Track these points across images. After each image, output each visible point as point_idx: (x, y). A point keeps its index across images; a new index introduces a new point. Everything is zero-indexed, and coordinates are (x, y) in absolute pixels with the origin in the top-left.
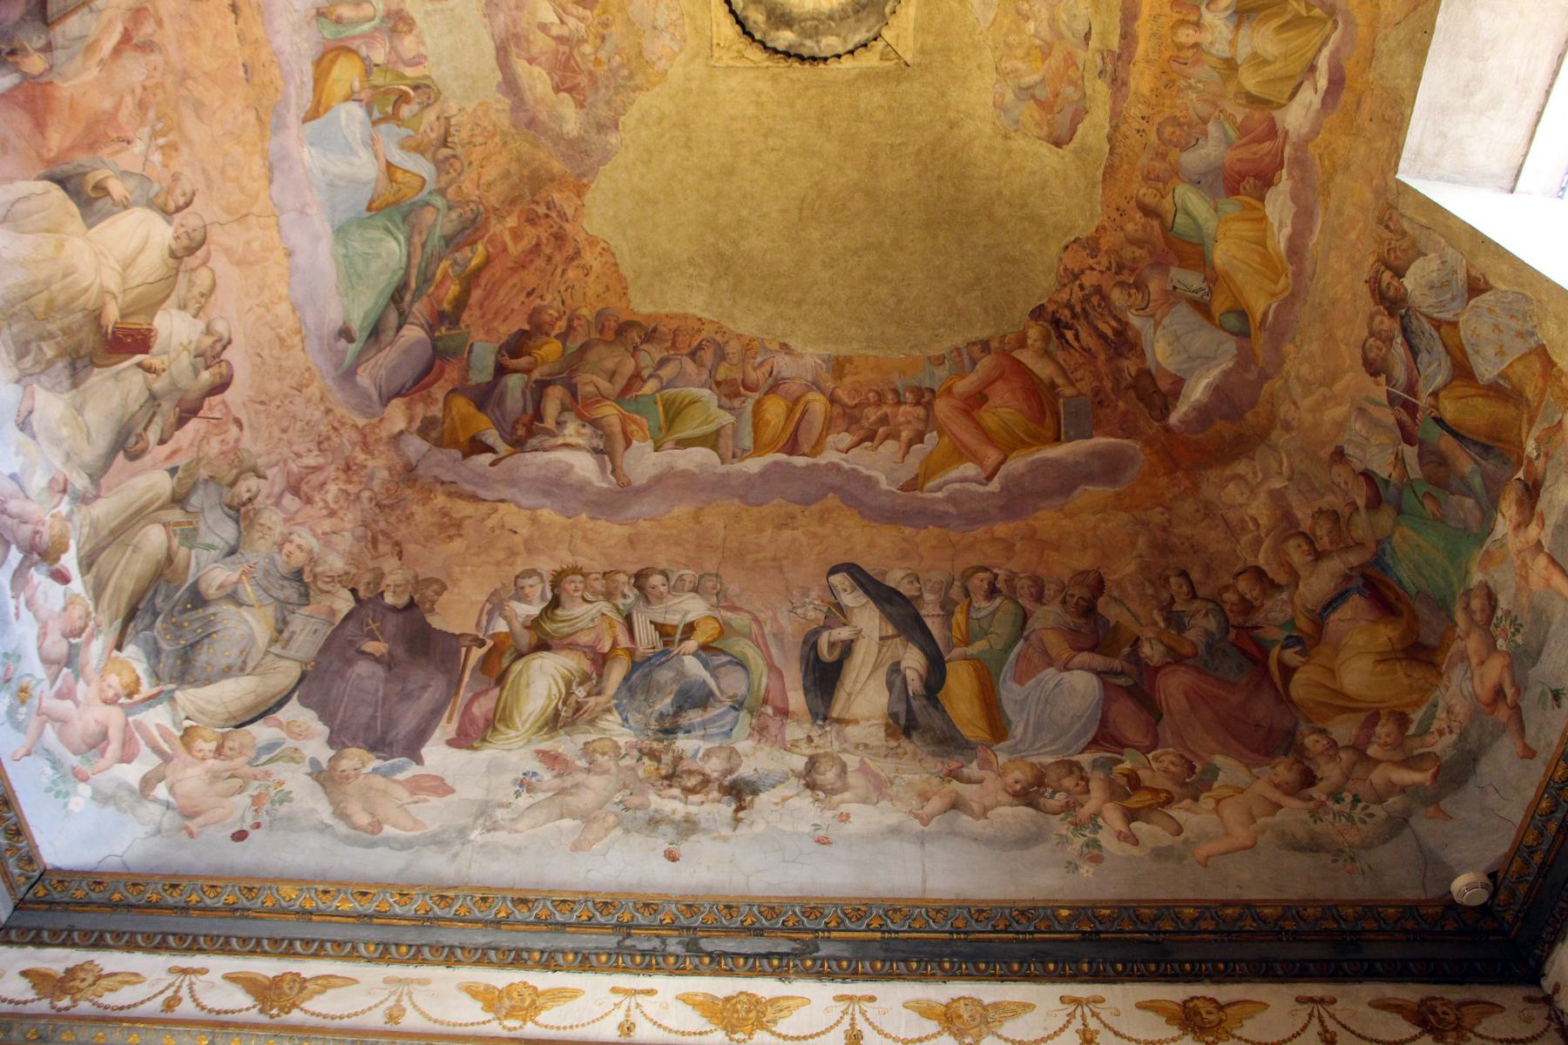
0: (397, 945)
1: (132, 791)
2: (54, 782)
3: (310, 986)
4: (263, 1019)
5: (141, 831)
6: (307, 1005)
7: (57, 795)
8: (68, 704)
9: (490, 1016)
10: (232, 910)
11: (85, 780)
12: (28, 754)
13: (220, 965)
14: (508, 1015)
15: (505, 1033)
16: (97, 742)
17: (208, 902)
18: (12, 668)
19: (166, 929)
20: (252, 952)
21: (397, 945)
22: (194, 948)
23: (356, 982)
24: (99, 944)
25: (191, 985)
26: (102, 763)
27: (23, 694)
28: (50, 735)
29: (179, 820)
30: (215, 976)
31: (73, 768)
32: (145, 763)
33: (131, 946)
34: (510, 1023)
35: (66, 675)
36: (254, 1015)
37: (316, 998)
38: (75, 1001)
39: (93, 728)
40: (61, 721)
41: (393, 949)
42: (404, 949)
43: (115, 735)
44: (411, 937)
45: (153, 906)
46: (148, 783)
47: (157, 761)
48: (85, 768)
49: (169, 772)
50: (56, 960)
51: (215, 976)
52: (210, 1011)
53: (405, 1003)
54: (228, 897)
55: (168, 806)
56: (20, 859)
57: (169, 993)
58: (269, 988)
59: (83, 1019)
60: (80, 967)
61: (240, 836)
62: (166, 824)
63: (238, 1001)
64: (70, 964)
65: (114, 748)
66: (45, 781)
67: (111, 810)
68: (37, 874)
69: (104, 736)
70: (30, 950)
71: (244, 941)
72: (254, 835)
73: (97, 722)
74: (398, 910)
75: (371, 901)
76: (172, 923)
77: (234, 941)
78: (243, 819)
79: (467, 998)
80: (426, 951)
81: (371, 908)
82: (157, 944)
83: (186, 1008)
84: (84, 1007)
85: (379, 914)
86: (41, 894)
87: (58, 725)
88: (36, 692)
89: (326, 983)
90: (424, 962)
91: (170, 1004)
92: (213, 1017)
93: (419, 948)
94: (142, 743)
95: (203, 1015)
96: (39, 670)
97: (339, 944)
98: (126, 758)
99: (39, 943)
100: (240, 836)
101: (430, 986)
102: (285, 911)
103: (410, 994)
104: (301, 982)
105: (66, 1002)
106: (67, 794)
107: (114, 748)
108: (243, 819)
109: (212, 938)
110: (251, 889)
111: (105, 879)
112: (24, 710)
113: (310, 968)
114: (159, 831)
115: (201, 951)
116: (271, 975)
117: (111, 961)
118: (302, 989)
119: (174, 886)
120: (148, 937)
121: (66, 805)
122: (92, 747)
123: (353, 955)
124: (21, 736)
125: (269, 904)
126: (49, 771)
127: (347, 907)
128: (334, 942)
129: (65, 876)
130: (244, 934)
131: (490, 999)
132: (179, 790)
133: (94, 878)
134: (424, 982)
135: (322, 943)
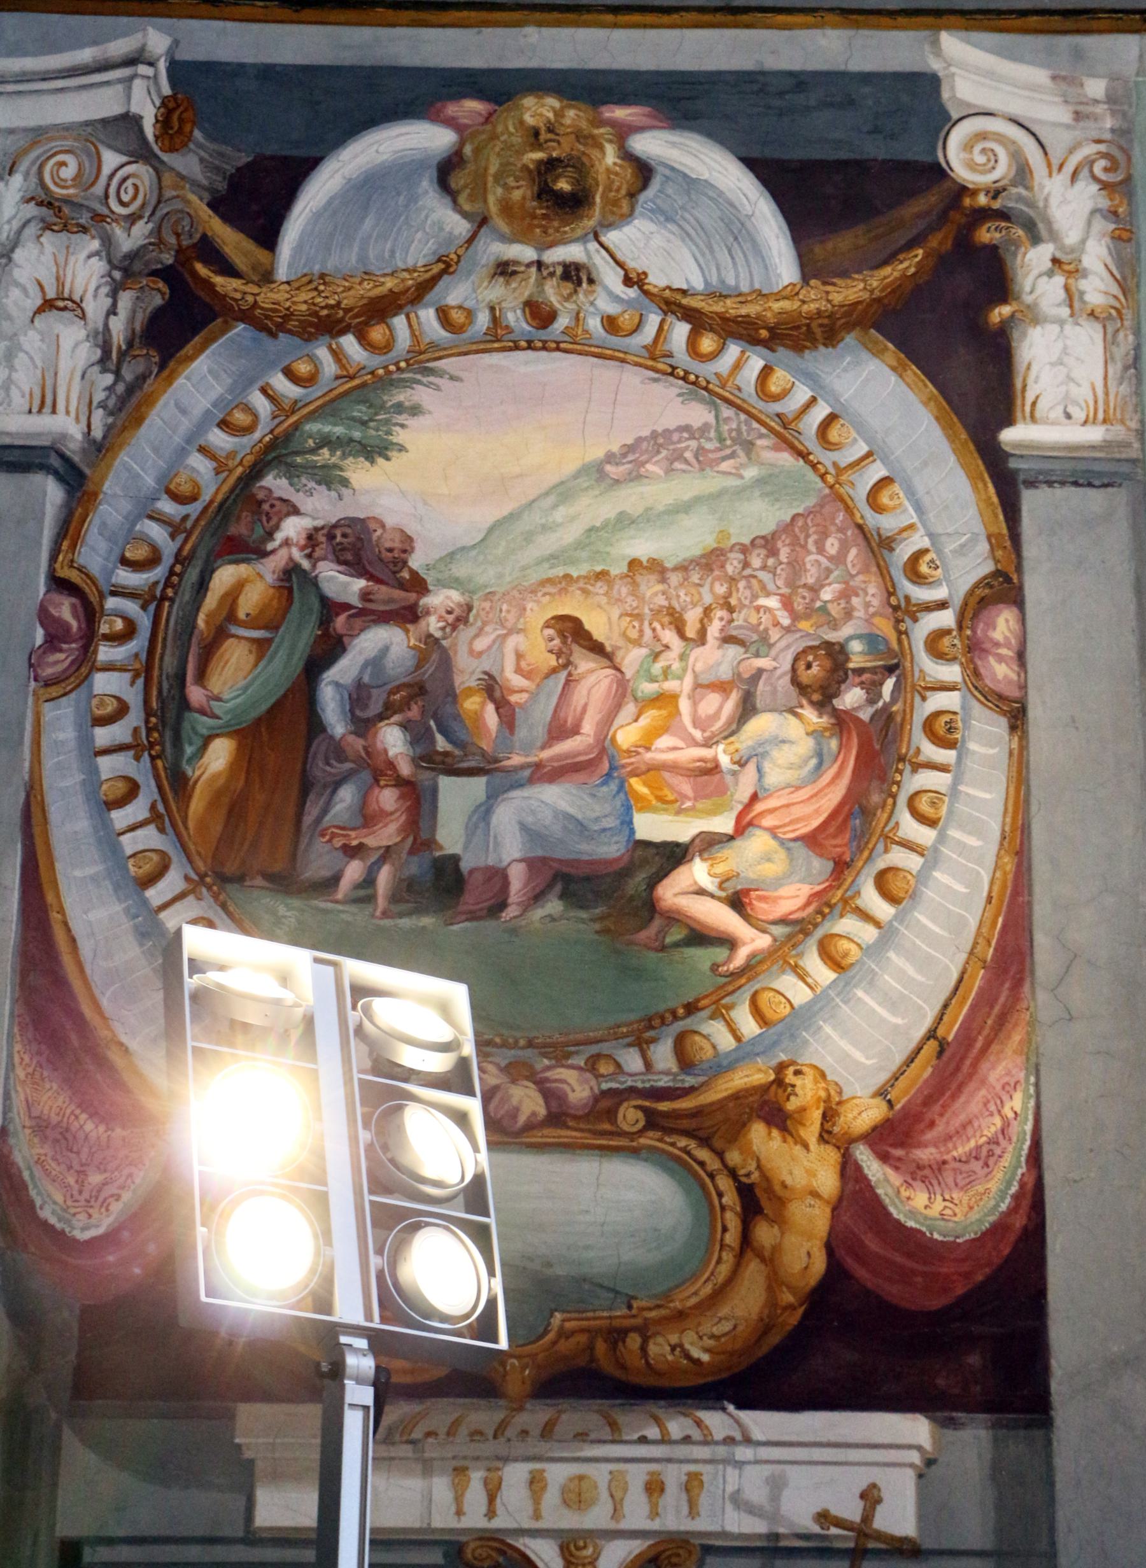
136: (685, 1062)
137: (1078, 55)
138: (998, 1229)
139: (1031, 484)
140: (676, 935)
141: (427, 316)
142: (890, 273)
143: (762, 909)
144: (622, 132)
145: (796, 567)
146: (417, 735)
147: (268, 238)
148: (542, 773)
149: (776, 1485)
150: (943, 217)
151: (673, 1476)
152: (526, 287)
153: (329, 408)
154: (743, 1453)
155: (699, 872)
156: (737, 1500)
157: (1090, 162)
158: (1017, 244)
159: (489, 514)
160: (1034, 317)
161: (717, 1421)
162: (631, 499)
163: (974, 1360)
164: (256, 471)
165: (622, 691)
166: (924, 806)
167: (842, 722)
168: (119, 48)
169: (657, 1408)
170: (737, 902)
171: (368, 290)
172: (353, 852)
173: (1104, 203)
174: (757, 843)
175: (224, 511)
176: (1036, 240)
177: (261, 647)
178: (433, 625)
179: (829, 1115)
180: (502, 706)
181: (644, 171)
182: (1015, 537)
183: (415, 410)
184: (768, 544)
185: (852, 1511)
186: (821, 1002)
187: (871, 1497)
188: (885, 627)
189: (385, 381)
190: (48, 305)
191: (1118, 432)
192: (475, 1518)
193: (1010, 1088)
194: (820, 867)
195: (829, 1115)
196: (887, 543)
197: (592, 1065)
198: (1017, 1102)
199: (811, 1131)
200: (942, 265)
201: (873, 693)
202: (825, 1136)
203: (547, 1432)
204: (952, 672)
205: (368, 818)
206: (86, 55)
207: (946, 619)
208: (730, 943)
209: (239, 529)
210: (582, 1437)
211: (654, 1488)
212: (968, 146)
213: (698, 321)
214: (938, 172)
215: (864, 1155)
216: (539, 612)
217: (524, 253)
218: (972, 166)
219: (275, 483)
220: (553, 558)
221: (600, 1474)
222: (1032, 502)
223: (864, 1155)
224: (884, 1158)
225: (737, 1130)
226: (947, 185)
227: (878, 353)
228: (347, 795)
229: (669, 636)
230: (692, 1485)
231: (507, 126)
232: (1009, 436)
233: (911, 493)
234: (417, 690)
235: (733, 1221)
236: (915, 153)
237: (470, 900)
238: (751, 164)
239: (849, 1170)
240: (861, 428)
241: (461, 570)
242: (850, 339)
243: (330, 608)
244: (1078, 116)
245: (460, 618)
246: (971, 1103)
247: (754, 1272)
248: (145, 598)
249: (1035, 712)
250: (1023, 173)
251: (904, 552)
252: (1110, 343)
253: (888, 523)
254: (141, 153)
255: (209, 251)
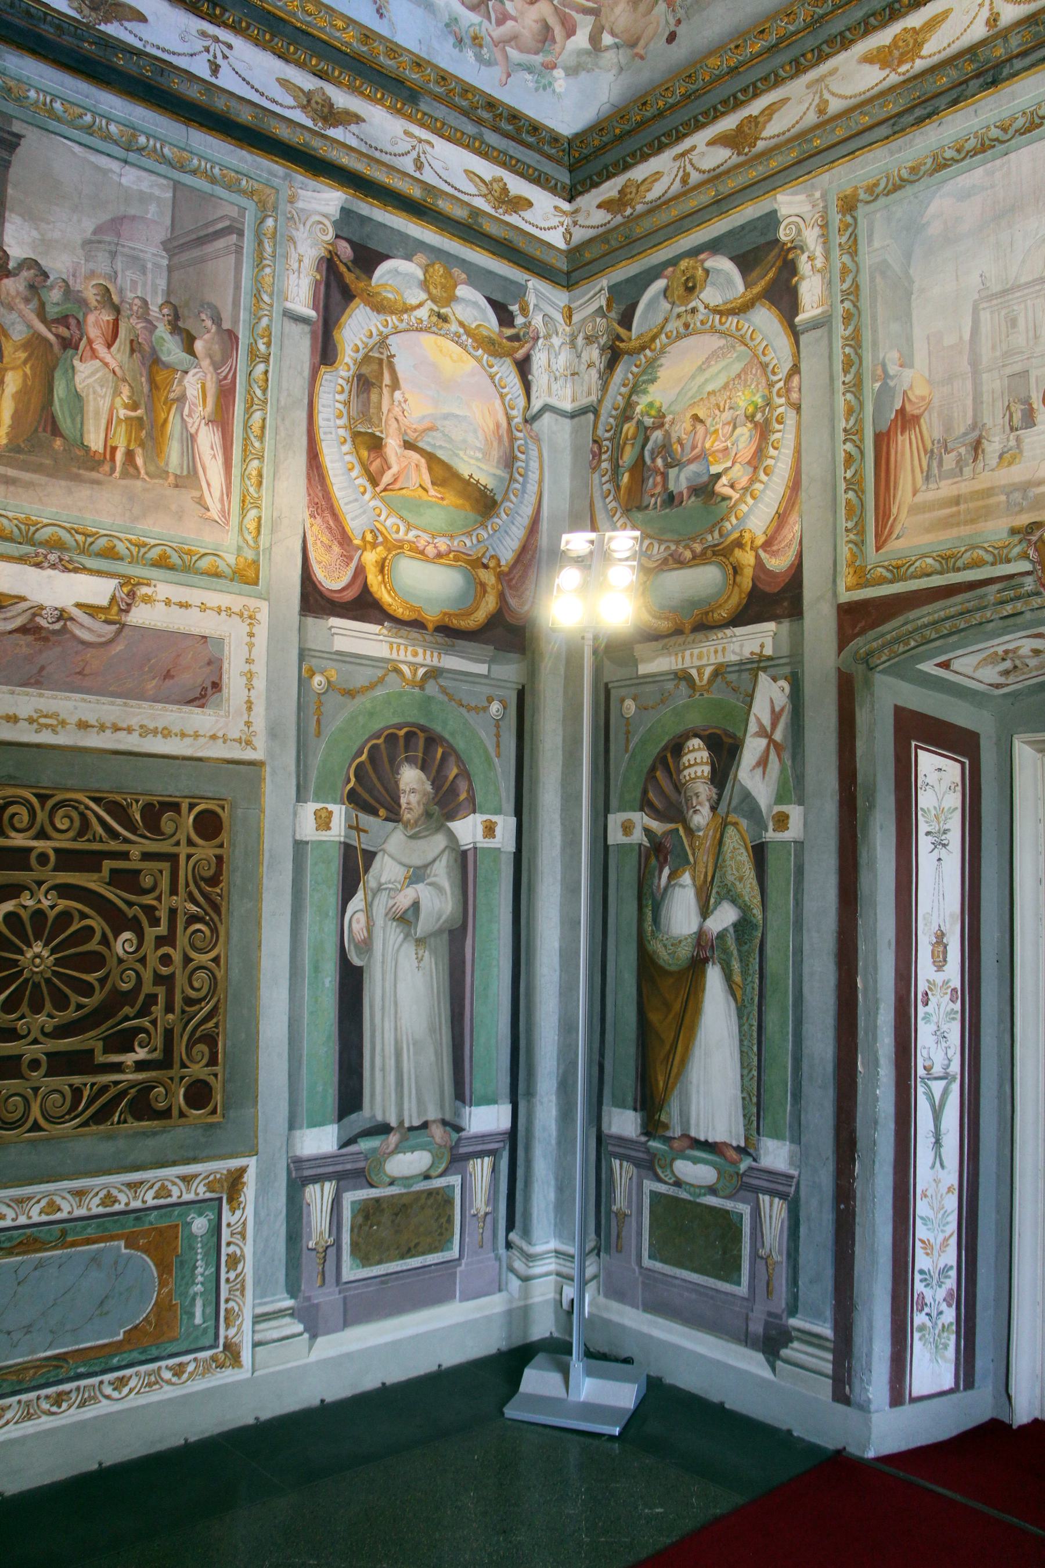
0: (803, 55)
1: (588, 53)
2: (537, 82)
3: (761, 119)
4: (742, 158)
5: (610, 76)
6: (764, 134)
7: (545, 88)
8: (510, 23)
9: (887, 71)
10: (688, 97)
11: (554, 67)
12: (509, 75)
13: (700, 138)
14: (901, 62)
15: (902, 78)
16: (546, 35)
17: (670, 101)
18: (457, 30)
19: (657, 134)
20: (716, 118)
21: (803, 55)
22: (680, 137)
23: (788, 99)
24: (627, 167)
25: (690, 160)
26: (557, 47)
27: (476, 41)
28: (513, 53)
29: (629, 52)
30: (701, 147)
31: (542, 64)
32: (585, 27)
33: (645, 157)
34: (903, 69)
35: (493, 7)
36: (736, 159)
37: (768, 126)
38: (633, 208)
39: (536, 27)
40: (513, 39)
41: (802, 60)
42: (809, 56)
43: (553, 21)
44: (811, 42)
45: (642, 124)
46: (595, 39)
47: (591, 19)
48: (549, 58)
49: (603, 22)
50: (610, 189)
51: (701, 147)
52: (709, 171)
53: (827, 96)
54: (680, 90)
55: (617, 46)
56: (549, 143)
57: (681, 174)
58: (737, 136)
59: (640, 216)
60: (625, 186)
61: (672, 38)
62: (623, 61)
63: (722, 155)
64: (619, 188)
65: (558, 31)
66: (531, 85)
67: (583, 75)
68: (566, 145)
69: (547, 28)
70: (594, 191)
71: (705, 114)
72: (681, 31)
73: (536, 22)
74: (792, 28)
75: (771, 34)
76: (659, 128)
77: (700, 118)
78: (667, 22)
79: (867, 68)
80: (825, 47)
81: (773, 39)
82: (658, 147)
83: (695, 177)
84: (640, 208)
85: (781, 40)
86: (577, 155)
87: (513, 43)
88: (484, 33)
89: (770, 111)
90: (829, 56)
91: (684, 181)
92: (713, 174)
93: (819, 48)
94: (573, 13)
95: (706, 176)
96: (474, 18)
97: (765, 79)
98: (570, 32)
99: (595, 185)
100: (672, 38)
101: (839, 73)
102: (720, 77)
103: (827, 86)
104: (753, 121)
105: (629, 211)
106: (550, 84)
107: (558, 31)
108: (667, 22)
109: (686, 124)
110: (690, 76)
111: (604, 125)
112: (485, 50)
113: (755, 107)
114: (621, 69)
115: (685, 135)
116: (734, 127)
117: (639, 172)
118: (757, 124)
119: (644, 104)
120: (650, 145)
121: (554, 91)
122: (544, 42)
123: (778, 82)
124: (497, 68)
125: (707, 78)
126: (529, 77)
127: (757, 47)
128: (760, 79)
129: (581, 137)
130: (703, 109)
131: (882, 58)
132: (617, 31)
133: (597, 128)
134: (833, 72)
135: (754, 84)
136: (721, 535)
137: (813, 186)
138: (792, 565)
139: (803, 333)
140: (719, 499)
141: (663, 336)
142: (767, 278)
143: (738, 486)
144: (703, 261)
145: (746, 381)
146: (664, 459)
147: (629, 329)
148: (690, 461)
149: (742, 646)
150: (779, 255)
151: (720, 648)
152: (683, 320)
153: (644, 372)
154: (734, 639)
155: (724, 480)
156: (734, 652)
157: (817, 220)
158: (798, 256)
159: (677, 390)
160: (802, 278)
161: (728, 632)
162: (707, 375)
163: (786, 604)
164: (630, 396)
165: (707, 431)
166: (775, 444)
167: (756, 424)
168: (597, 289)
169: (715, 631)
170: (732, 486)
171: (651, 334)
172: (652, 496)
173: (821, 232)
174: (737, 466)
175: (625, 410)
176: (803, 252)
177: (633, 444)
178: (667, 426)
179: (752, 542)
180: (682, 445)
181: (707, 272)
182: (799, 352)
183: (661, 366)
184: (739, 376)
185: (757, 650)
186: (750, 510)
187: (762, 646)
188: (766, 392)
189: (655, 359)
190: (589, 366)
191: (826, 307)
192: (680, 666)
193: (794, 524)
194: (751, 470)
195: (752, 542)
196: (767, 365)
197: (701, 542)
198: (797, 527)
199: (748, 548)
200: (780, 270)
201: (763, 412)
202: (752, 548)
203: (693, 642)
204: (782, 401)
205: (655, 485)
206: (592, 293)
207: (781, 384)
208: (730, 498)
209: (628, 414)
210: (701, 641)
211: (716, 652)
212: (785, 229)
213: (721, 313)
214: (777, 241)
215: (761, 552)
216: (689, 415)
217: (683, 309)
218: (786, 235)
219: (634, 398)
220: (692, 398)
221: (705, 650)
222: (803, 339)
223: (761, 552)
224: (765, 551)
225: (732, 551)
226: (780, 245)
227: (763, 306)
228: (651, 480)
229: (717, 412)
230: (724, 649)
231: (678, 273)
232: (797, 319)
233: (772, 347)
234: (664, 446)
235: (731, 577)
236: (770, 237)
237: (676, 502)
238: (731, 259)
239: (757, 557)
240: (761, 332)
241: (672, 409)
242: (757, 304)
243: (646, 428)
244: (813, 206)
245: (673, 423)
246: (785, 531)
247: (736, 589)
248: (610, 439)
249: (803, 406)
250: (799, 232)
251: (771, 367)
252: (823, 278)
253: (764, 359)
254: (604, 316)
255: (618, 338)
